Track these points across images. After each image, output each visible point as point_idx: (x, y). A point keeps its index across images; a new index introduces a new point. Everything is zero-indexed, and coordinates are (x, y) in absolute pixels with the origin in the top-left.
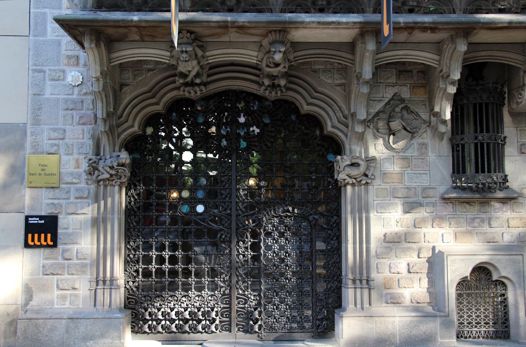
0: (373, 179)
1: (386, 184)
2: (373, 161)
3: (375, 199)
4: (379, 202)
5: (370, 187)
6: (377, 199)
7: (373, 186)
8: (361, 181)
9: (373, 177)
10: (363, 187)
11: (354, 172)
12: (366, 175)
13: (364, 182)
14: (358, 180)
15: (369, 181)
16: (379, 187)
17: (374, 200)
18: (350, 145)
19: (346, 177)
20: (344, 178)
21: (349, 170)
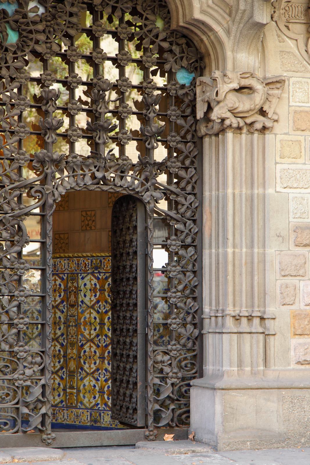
0: (276, 121)
1: (299, 133)
2: (278, 85)
3: (278, 160)
4: (286, 166)
5: (269, 136)
6: (283, 161)
7: (276, 134)
8: (252, 124)
9: (275, 117)
10: (256, 135)
11: (244, 104)
12: (262, 112)
13: (258, 126)
14: (249, 121)
15: (268, 124)
16: (286, 137)
17: (276, 163)
18: (233, 51)
19: (229, 115)
20: (224, 116)
21: (233, 100)
